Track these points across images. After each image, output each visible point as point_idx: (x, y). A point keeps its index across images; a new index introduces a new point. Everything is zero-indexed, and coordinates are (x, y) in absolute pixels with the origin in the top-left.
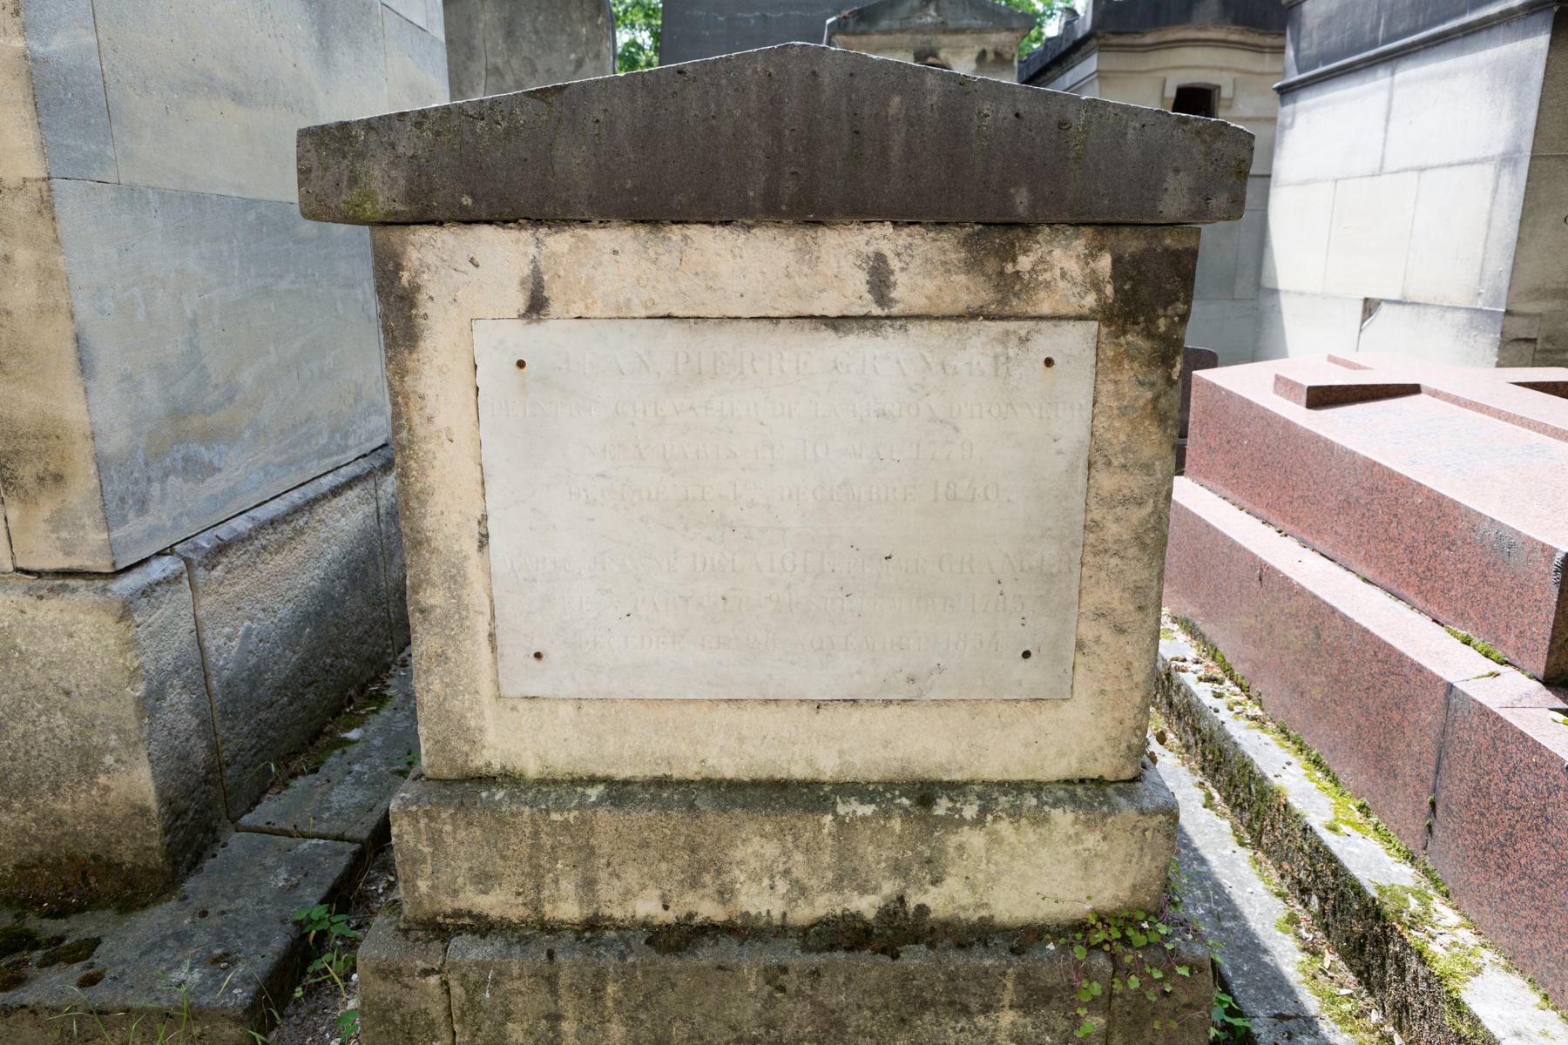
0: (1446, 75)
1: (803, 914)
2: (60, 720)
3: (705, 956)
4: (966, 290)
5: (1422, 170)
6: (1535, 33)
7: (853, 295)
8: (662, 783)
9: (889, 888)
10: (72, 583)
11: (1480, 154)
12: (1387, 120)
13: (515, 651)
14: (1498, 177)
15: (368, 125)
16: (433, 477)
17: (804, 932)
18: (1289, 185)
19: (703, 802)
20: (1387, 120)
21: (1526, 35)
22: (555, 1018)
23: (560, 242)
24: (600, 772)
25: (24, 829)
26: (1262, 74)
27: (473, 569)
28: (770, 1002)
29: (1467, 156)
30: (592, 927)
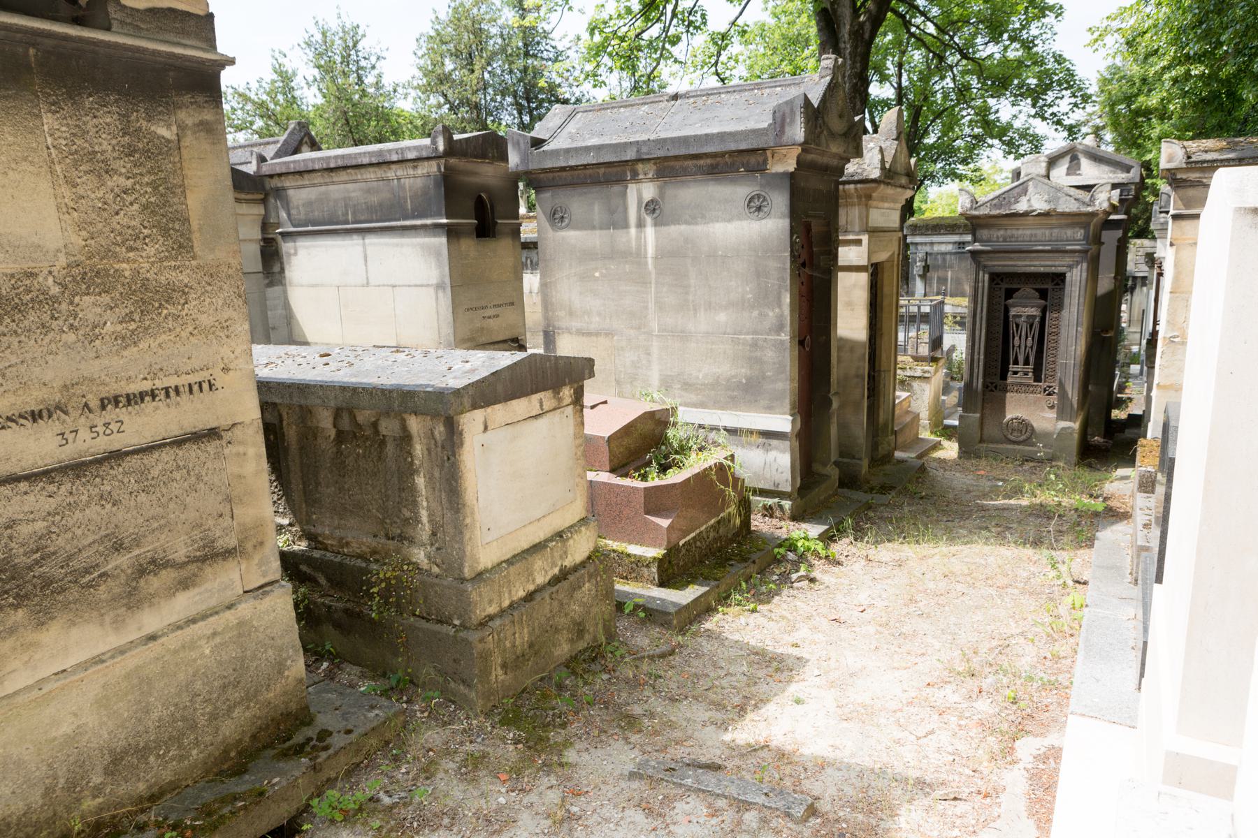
0: (397, 245)
1: (547, 580)
2: (270, 652)
3: (538, 597)
4: (553, 403)
5: (394, 286)
7: (537, 411)
8: (514, 556)
9: (560, 564)
10: (266, 589)
11: (425, 283)
12: (366, 261)
13: (485, 530)
14: (437, 293)
15: (463, 388)
16: (467, 484)
17: (549, 583)
18: (302, 286)
19: (525, 555)
20: (366, 261)
21: (435, 236)
22: (514, 634)
23: (489, 410)
25: (255, 716)
26: (242, 215)
27: (476, 510)
29: (419, 283)
30: (511, 606)
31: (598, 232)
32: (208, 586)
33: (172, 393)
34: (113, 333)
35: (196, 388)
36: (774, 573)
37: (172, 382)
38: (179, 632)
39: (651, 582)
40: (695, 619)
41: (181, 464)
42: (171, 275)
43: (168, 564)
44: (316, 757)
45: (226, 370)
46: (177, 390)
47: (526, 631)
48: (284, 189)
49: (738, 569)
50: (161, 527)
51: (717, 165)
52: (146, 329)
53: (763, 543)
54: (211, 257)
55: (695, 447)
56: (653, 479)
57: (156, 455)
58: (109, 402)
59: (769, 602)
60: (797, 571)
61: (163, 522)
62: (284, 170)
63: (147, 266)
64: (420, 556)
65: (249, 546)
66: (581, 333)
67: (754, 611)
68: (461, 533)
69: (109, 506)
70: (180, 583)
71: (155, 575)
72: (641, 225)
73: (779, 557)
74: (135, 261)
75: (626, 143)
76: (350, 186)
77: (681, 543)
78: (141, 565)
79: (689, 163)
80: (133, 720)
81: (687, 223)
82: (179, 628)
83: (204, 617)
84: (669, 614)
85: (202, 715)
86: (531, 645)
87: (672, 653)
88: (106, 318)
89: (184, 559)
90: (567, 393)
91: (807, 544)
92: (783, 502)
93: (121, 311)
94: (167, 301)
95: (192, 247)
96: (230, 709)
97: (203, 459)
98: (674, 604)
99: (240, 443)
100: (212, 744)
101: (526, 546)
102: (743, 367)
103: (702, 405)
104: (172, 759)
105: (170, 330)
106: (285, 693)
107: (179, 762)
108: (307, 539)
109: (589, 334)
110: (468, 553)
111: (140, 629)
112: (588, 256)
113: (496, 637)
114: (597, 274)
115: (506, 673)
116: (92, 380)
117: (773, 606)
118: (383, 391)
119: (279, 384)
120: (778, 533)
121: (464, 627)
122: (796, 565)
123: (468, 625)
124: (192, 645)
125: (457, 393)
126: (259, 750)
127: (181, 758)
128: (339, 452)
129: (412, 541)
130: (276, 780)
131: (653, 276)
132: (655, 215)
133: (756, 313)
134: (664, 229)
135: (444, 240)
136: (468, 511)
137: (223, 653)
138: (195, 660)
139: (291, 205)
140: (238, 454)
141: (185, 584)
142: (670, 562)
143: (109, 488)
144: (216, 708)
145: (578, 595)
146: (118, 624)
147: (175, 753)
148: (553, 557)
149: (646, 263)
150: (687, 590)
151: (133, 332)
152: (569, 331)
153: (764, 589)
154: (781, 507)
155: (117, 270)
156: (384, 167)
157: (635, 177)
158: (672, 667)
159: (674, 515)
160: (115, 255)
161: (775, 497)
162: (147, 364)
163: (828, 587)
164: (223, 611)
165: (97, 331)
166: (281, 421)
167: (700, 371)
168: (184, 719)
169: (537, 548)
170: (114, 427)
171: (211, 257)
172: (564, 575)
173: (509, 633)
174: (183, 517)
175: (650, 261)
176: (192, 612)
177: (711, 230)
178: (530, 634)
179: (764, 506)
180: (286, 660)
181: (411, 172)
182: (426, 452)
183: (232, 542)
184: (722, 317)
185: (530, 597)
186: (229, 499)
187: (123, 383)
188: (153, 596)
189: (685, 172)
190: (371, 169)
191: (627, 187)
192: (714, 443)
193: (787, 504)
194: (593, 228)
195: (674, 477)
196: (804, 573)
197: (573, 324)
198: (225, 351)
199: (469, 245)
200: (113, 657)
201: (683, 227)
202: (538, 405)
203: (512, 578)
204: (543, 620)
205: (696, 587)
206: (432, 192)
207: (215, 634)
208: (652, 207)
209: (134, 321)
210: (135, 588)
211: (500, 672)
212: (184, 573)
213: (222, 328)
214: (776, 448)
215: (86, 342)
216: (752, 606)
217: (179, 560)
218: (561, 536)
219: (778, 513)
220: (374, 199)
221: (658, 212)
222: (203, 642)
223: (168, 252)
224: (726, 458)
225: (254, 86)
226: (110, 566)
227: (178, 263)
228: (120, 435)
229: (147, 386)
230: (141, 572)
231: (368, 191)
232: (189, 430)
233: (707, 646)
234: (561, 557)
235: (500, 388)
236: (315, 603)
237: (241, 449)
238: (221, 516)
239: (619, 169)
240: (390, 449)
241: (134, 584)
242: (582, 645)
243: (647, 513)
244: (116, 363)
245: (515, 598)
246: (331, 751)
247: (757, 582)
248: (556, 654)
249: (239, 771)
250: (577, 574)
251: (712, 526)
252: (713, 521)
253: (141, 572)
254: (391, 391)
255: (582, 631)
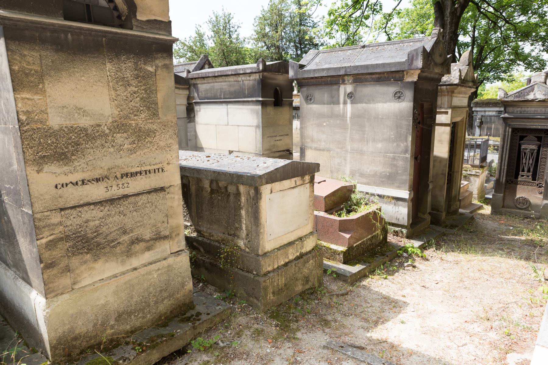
0: (241, 109)
3: (290, 265)
4: (301, 182)
5: (239, 126)
6: (258, 105)
7: (294, 185)
8: (281, 247)
9: (300, 251)
10: (179, 253)
11: (251, 125)
12: (228, 115)
14: (256, 130)
15: (263, 175)
18: (202, 124)
19: (285, 247)
20: (228, 115)
21: (256, 105)
22: (278, 280)
23: (273, 184)
24: (276, 247)
28: (295, 268)
30: (278, 268)
31: (326, 106)
32: (157, 250)
33: (148, 173)
34: (127, 148)
35: (157, 171)
36: (396, 262)
37: (148, 168)
38: (145, 268)
39: (340, 262)
40: (358, 280)
41: (150, 201)
42: (150, 126)
43: (142, 240)
44: (195, 323)
45: (168, 164)
46: (150, 171)
47: (283, 279)
48: (197, 84)
49: (380, 259)
50: (141, 225)
51: (381, 77)
52: (139, 147)
53: (393, 248)
54: (165, 118)
55: (363, 203)
56: (343, 216)
57: (140, 197)
58: (124, 176)
59: (393, 275)
60: (407, 262)
61: (142, 223)
62: (197, 77)
63: (141, 122)
64: (241, 243)
65: (174, 235)
66: (316, 149)
67: (386, 278)
68: (259, 235)
69: (122, 216)
70: (147, 248)
71: (138, 244)
72: (345, 103)
73: (399, 255)
74: (137, 120)
75: (340, 67)
76: (223, 83)
77: (354, 245)
78: (133, 240)
79: (368, 76)
80: (127, 301)
81: (366, 103)
82: (146, 266)
83: (155, 262)
84: (347, 276)
85: (152, 301)
86: (285, 285)
87: (347, 294)
88: (125, 142)
89: (149, 239)
90: (307, 178)
91: (413, 250)
92: (403, 230)
93: (131, 140)
94: (148, 136)
95: (158, 114)
96: (163, 300)
97: (158, 199)
98: (349, 272)
99: (173, 193)
100: (155, 313)
101: (286, 242)
102: (388, 168)
103: (368, 184)
104: (140, 318)
105: (148, 148)
106: (184, 295)
107: (143, 319)
108: (197, 232)
109: (320, 150)
110: (261, 244)
111: (131, 265)
112: (321, 116)
113: (271, 280)
114: (325, 124)
115: (274, 296)
116: (119, 167)
117: (395, 277)
118: (230, 174)
119: (189, 168)
120: (400, 244)
121: (257, 275)
122: (407, 259)
123: (259, 274)
124: (150, 273)
125: (260, 177)
126: (173, 318)
127: (144, 318)
128: (211, 198)
129: (238, 237)
130: (179, 331)
131: (349, 126)
132: (352, 99)
133: (395, 144)
134: (355, 105)
135: (260, 107)
136: (262, 226)
137: (161, 277)
138: (151, 279)
139: (199, 91)
140: (171, 198)
141: (148, 249)
142: (349, 253)
143: (122, 209)
144: (158, 299)
145: (307, 265)
146: (123, 262)
147: (142, 315)
148: (297, 248)
149: (347, 120)
150: (356, 266)
151: (134, 148)
152: (311, 148)
153: (391, 269)
154: (402, 232)
155: (130, 124)
156: (237, 76)
157: (344, 82)
158: (346, 300)
159: (352, 233)
160: (130, 118)
161: (399, 227)
162: (139, 161)
163: (421, 270)
164: (162, 260)
165: (121, 147)
166: (189, 183)
167: (368, 169)
168: (145, 302)
169: (290, 244)
170: (126, 185)
171: (165, 118)
172: (301, 256)
173: (276, 279)
174: (149, 222)
175: (348, 119)
176: (151, 260)
177: (377, 106)
178: (285, 280)
179: (394, 231)
180: (185, 282)
181: (248, 78)
182: (246, 201)
183: (167, 233)
184: (380, 145)
185: (286, 265)
186: (167, 216)
187: (130, 168)
188: (136, 252)
189: (366, 80)
190: (232, 77)
191: (340, 86)
192: (372, 201)
193: (405, 231)
194: (324, 104)
195: (353, 216)
196: (410, 263)
197: (313, 145)
198: (169, 156)
199: (271, 110)
200: (120, 275)
201: (364, 105)
202: (294, 183)
203: (279, 256)
204: (291, 275)
205: (360, 265)
206: (256, 87)
207: (159, 269)
208: (350, 96)
209: (135, 143)
210: (130, 249)
211: (271, 295)
212: (148, 244)
213: (168, 147)
214: (401, 205)
215: (117, 152)
216: (385, 276)
217: (147, 239)
218: (301, 239)
219: (400, 235)
220: (232, 89)
221: (353, 98)
222: (154, 272)
223: (149, 116)
224: (377, 209)
225: (188, 39)
226: (121, 240)
227: (153, 121)
228: (127, 188)
229: (138, 169)
230: (133, 243)
231: (230, 86)
232: (153, 187)
233: (363, 292)
234: (301, 248)
235: (278, 175)
236: (198, 259)
237: (173, 196)
238: (163, 222)
239: (337, 78)
240: (232, 198)
241: (130, 247)
242: (307, 287)
243: (340, 231)
244: (128, 160)
245: (280, 265)
246: (201, 321)
247: (388, 266)
248: (296, 289)
249: (165, 325)
250: (307, 256)
251: (369, 239)
252: (369, 237)
253: (133, 243)
254: (233, 175)
255: (308, 281)
